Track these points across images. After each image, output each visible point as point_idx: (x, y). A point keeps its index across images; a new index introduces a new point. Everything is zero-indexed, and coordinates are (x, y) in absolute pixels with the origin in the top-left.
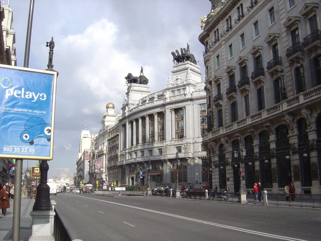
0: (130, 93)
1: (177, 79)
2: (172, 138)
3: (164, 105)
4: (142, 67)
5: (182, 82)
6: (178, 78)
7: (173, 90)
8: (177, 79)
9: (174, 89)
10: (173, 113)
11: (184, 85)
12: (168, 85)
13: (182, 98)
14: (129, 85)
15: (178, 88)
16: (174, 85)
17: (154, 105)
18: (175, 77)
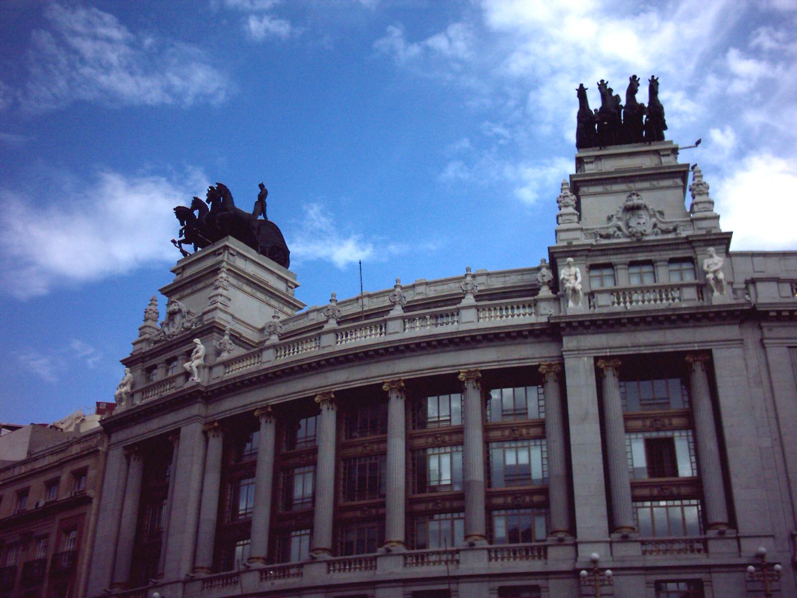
0: (224, 275)
1: (632, 210)
2: (613, 527)
3: (553, 331)
4: (261, 186)
5: (663, 227)
6: (635, 201)
7: (602, 260)
8: (632, 210)
9: (613, 259)
10: (611, 381)
11: (689, 242)
12: (562, 236)
13: (688, 299)
14: (189, 248)
15: (641, 257)
16: (608, 236)
17: (463, 328)
18: (621, 200)
